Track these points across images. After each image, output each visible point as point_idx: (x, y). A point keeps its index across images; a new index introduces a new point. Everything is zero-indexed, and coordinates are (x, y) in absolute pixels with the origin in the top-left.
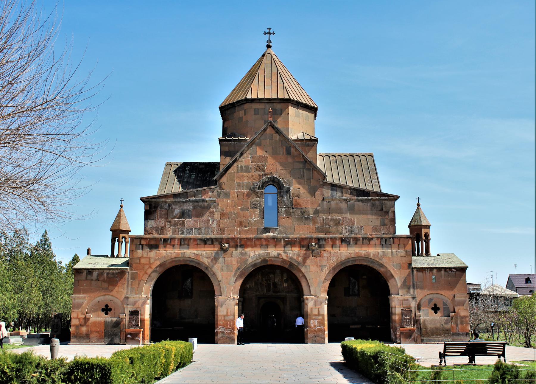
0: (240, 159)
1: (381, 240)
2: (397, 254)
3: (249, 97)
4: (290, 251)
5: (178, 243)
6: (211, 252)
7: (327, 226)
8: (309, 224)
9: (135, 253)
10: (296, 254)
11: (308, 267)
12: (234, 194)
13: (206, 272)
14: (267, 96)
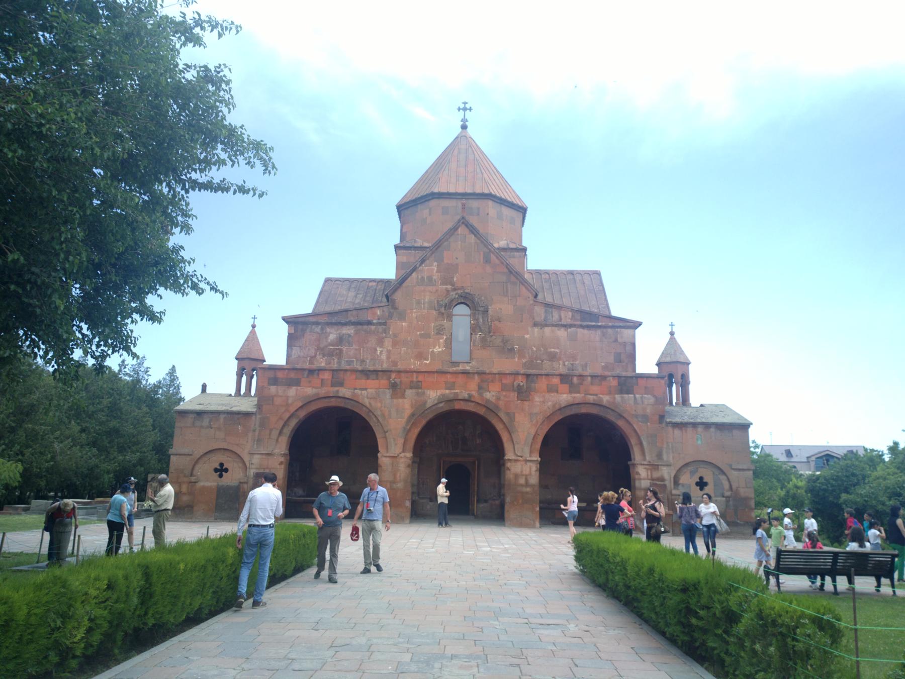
2: (642, 402)
3: (436, 191)
7: (538, 361)
8: (514, 358)
14: (461, 190)
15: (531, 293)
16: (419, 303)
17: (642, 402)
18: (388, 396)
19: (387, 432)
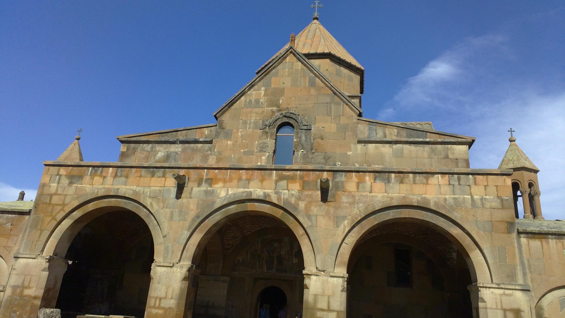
0: (249, 92)
1: (449, 177)
2: (483, 204)
4: (285, 190)
5: (112, 173)
6: (160, 188)
9: (46, 188)
10: (295, 196)
11: (313, 219)
12: (238, 134)
13: (147, 221)
15: (354, 112)
16: (245, 123)
17: (483, 204)
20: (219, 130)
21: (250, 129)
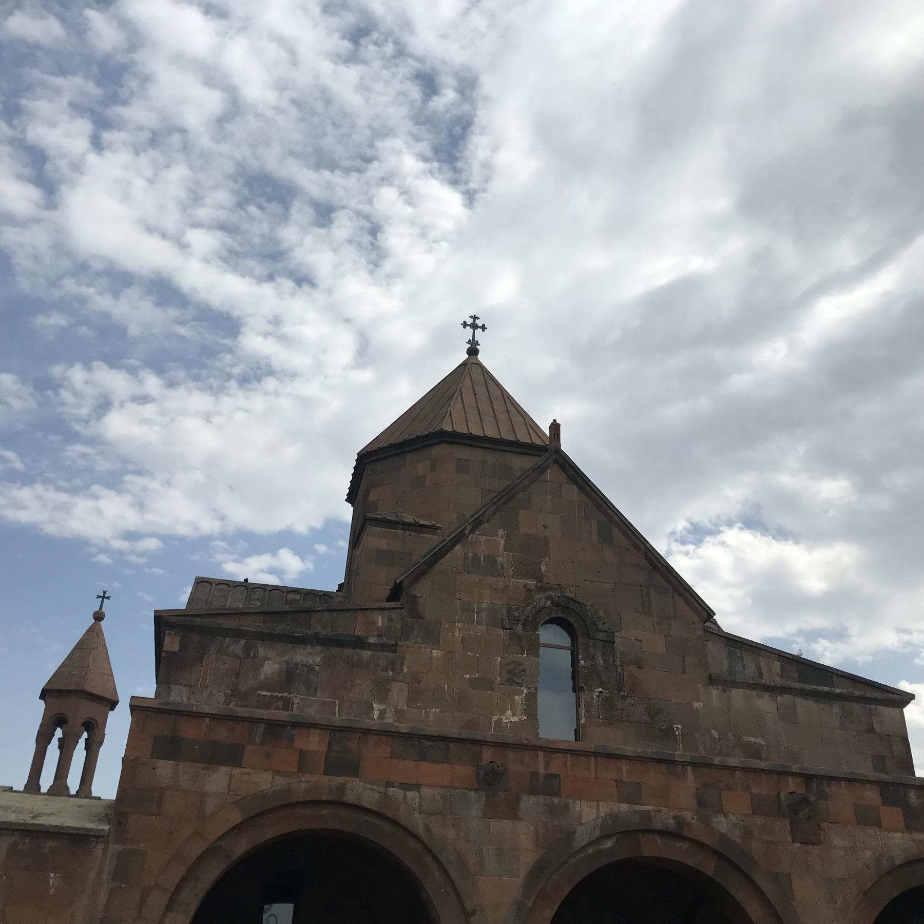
0: (471, 535)
18: (476, 811)
19: (474, 913)
20: (409, 620)
21: (482, 625)
